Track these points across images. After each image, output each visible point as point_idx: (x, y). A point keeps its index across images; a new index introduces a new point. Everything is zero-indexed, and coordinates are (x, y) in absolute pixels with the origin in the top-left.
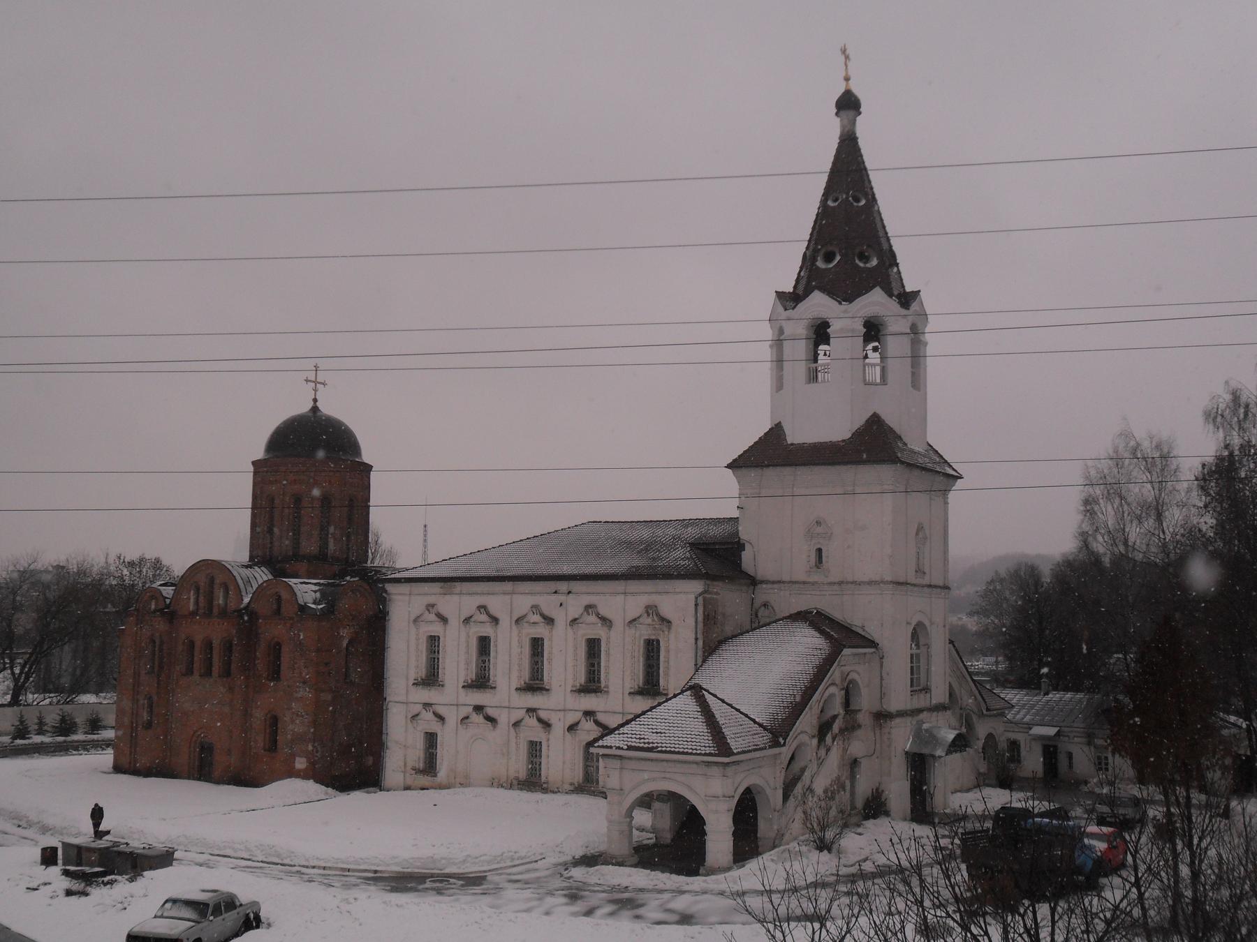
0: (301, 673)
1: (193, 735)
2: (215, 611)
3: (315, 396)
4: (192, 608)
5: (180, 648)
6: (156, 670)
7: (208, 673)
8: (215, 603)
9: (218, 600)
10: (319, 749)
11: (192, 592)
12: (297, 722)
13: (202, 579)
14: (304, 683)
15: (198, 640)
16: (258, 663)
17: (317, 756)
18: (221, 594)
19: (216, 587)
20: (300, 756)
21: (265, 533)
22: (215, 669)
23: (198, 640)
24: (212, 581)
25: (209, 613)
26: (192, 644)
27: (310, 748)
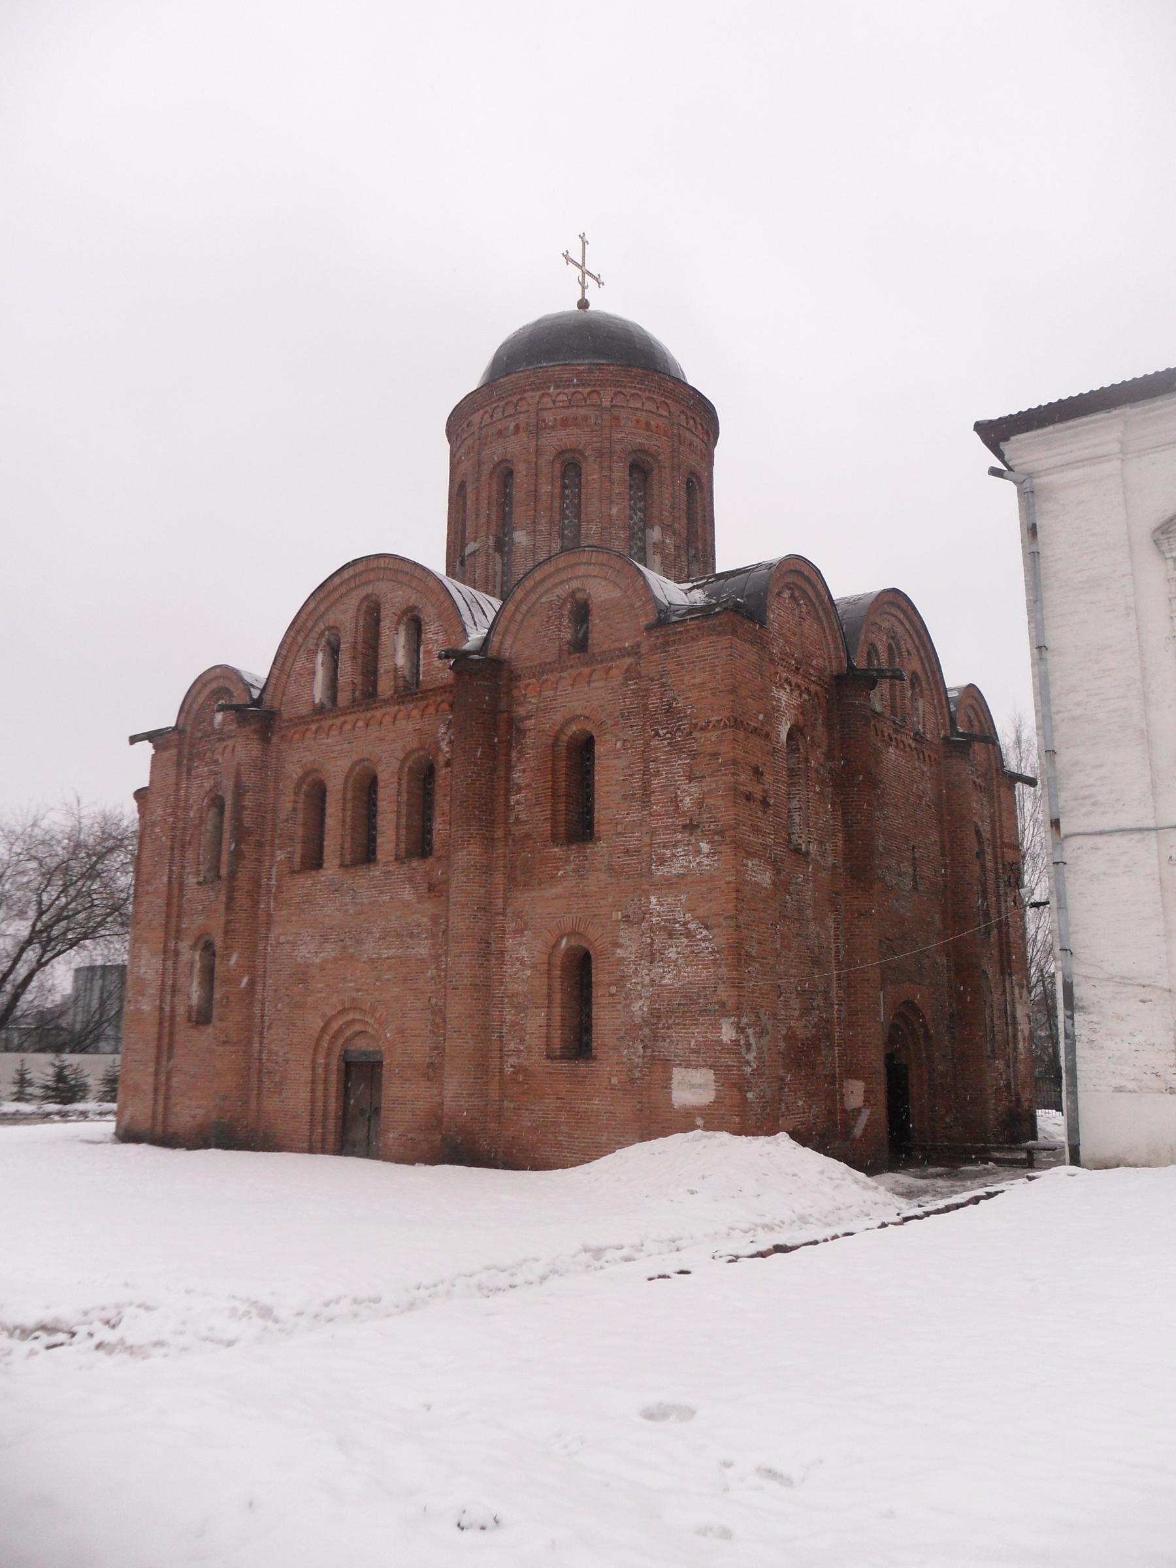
0: (675, 801)
1: (324, 1029)
2: (385, 687)
3: (583, 293)
4: (319, 693)
5: (287, 803)
6: (224, 872)
7: (366, 854)
8: (384, 665)
9: (394, 655)
10: (752, 1040)
11: (320, 658)
12: (672, 954)
13: (346, 617)
14: (691, 827)
15: (336, 778)
16: (518, 803)
17: (748, 1063)
18: (401, 640)
19: (386, 624)
20: (688, 1066)
21: (491, 551)
22: (387, 841)
23: (336, 778)
24: (373, 612)
25: (368, 695)
26: (317, 795)
27: (727, 1033)
